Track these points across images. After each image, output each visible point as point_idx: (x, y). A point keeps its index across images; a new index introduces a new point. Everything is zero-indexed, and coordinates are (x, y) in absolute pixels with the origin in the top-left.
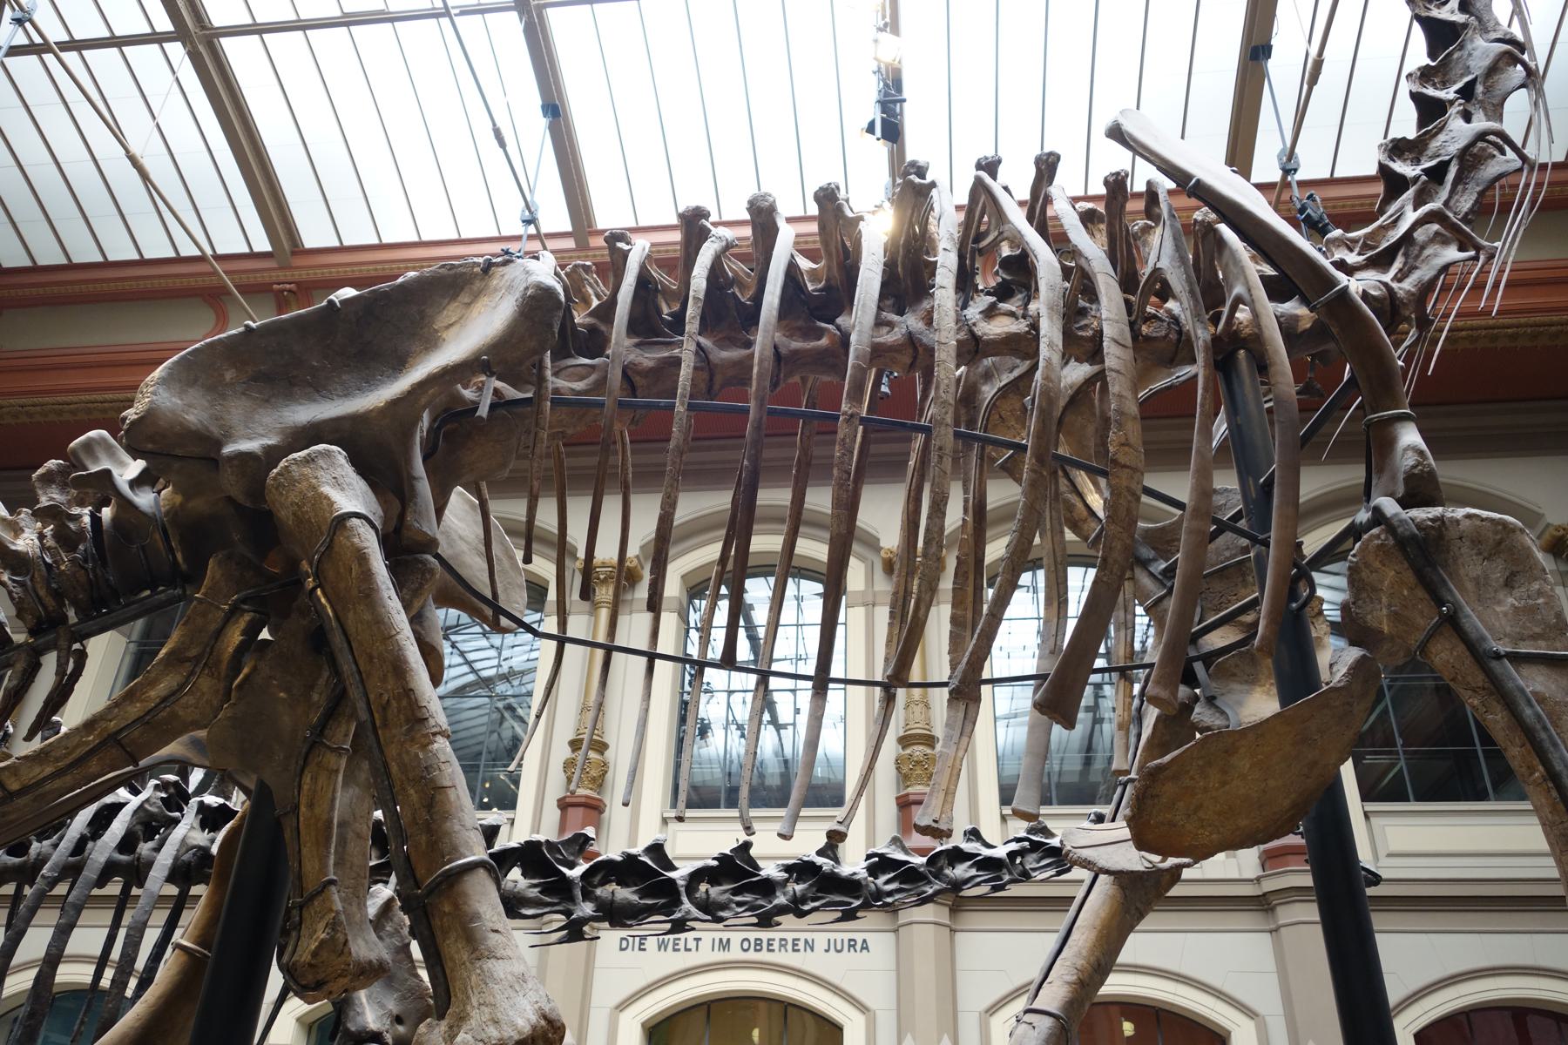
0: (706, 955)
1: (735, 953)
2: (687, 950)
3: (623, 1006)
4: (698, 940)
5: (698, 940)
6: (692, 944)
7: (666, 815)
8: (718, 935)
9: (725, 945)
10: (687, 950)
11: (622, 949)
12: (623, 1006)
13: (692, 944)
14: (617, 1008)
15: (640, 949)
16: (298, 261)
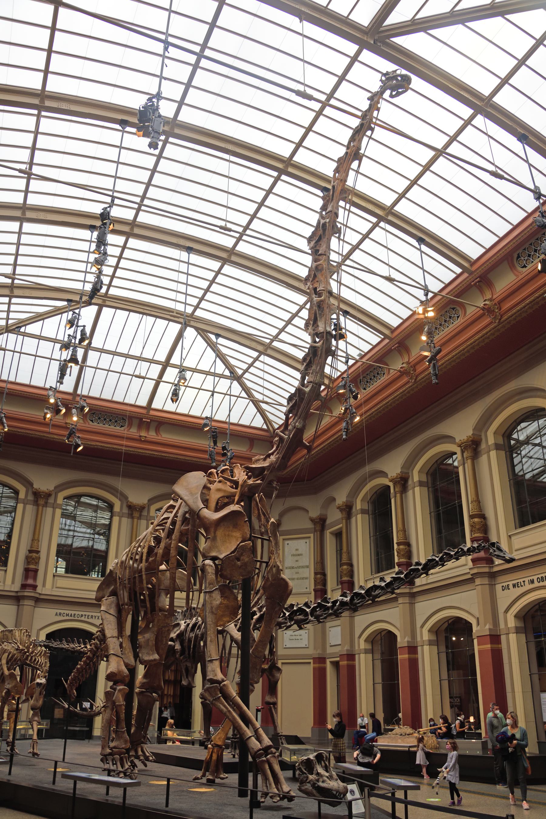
0: (528, 587)
1: (536, 584)
2: (522, 586)
3: (507, 611)
4: (524, 581)
5: (524, 581)
6: (522, 584)
7: (509, 534)
8: (529, 578)
9: (532, 582)
10: (522, 586)
11: (503, 590)
12: (507, 611)
13: (522, 584)
14: (505, 612)
15: (509, 589)
16: (335, 384)
